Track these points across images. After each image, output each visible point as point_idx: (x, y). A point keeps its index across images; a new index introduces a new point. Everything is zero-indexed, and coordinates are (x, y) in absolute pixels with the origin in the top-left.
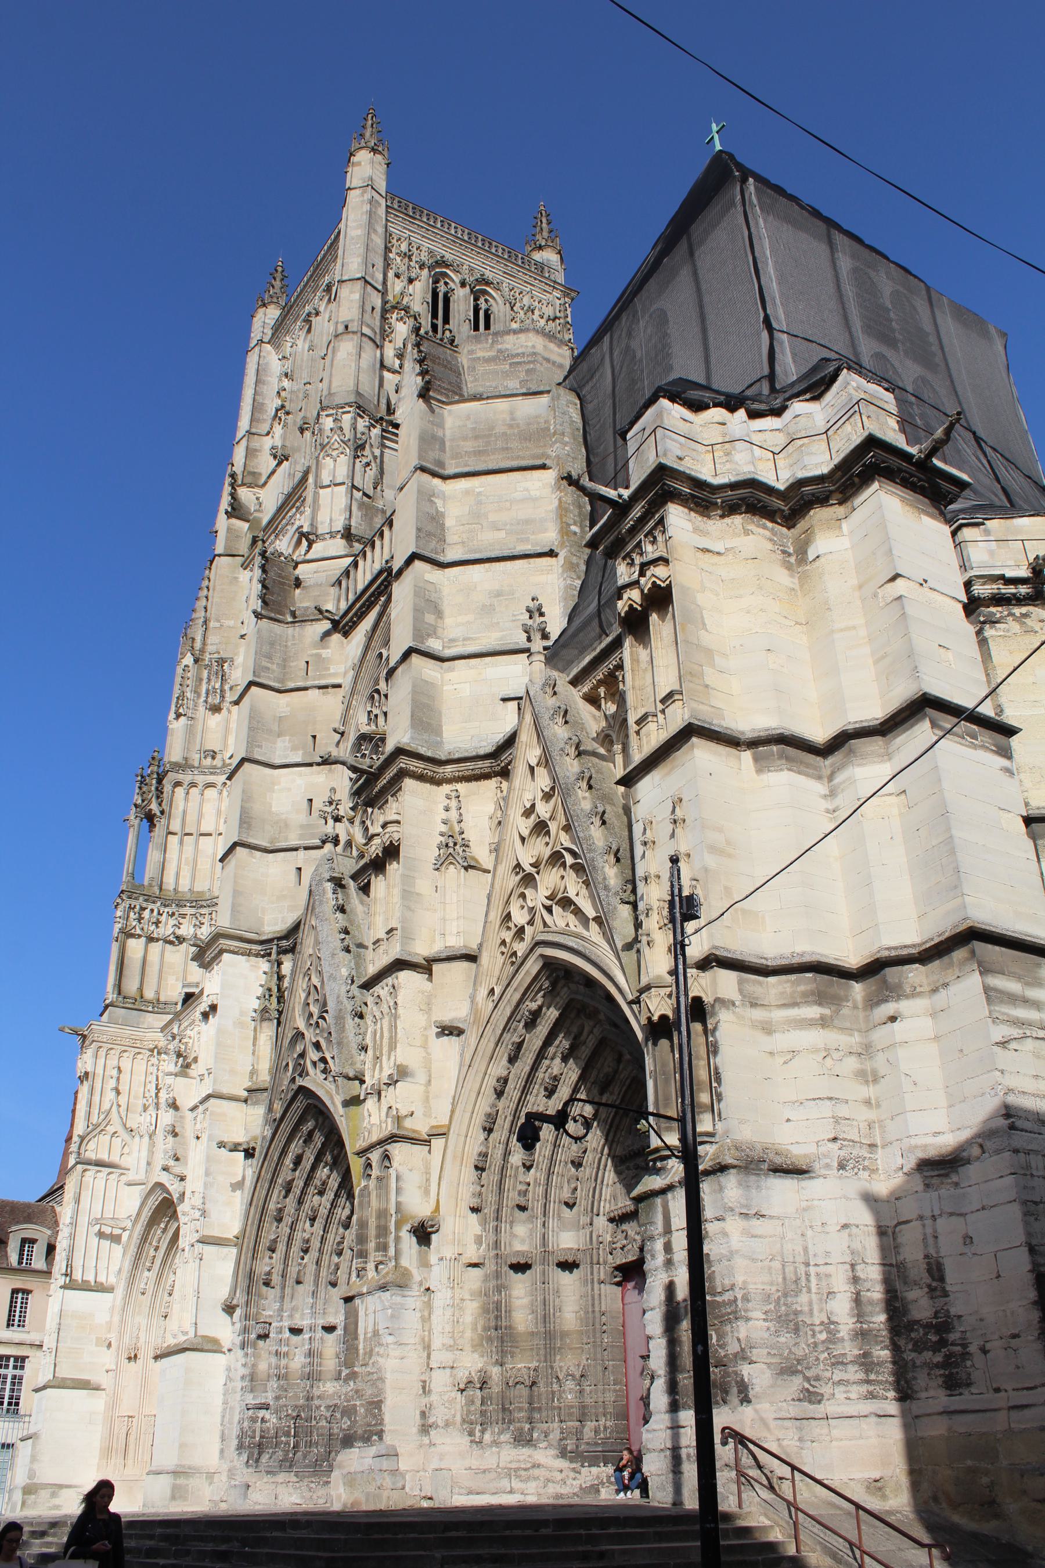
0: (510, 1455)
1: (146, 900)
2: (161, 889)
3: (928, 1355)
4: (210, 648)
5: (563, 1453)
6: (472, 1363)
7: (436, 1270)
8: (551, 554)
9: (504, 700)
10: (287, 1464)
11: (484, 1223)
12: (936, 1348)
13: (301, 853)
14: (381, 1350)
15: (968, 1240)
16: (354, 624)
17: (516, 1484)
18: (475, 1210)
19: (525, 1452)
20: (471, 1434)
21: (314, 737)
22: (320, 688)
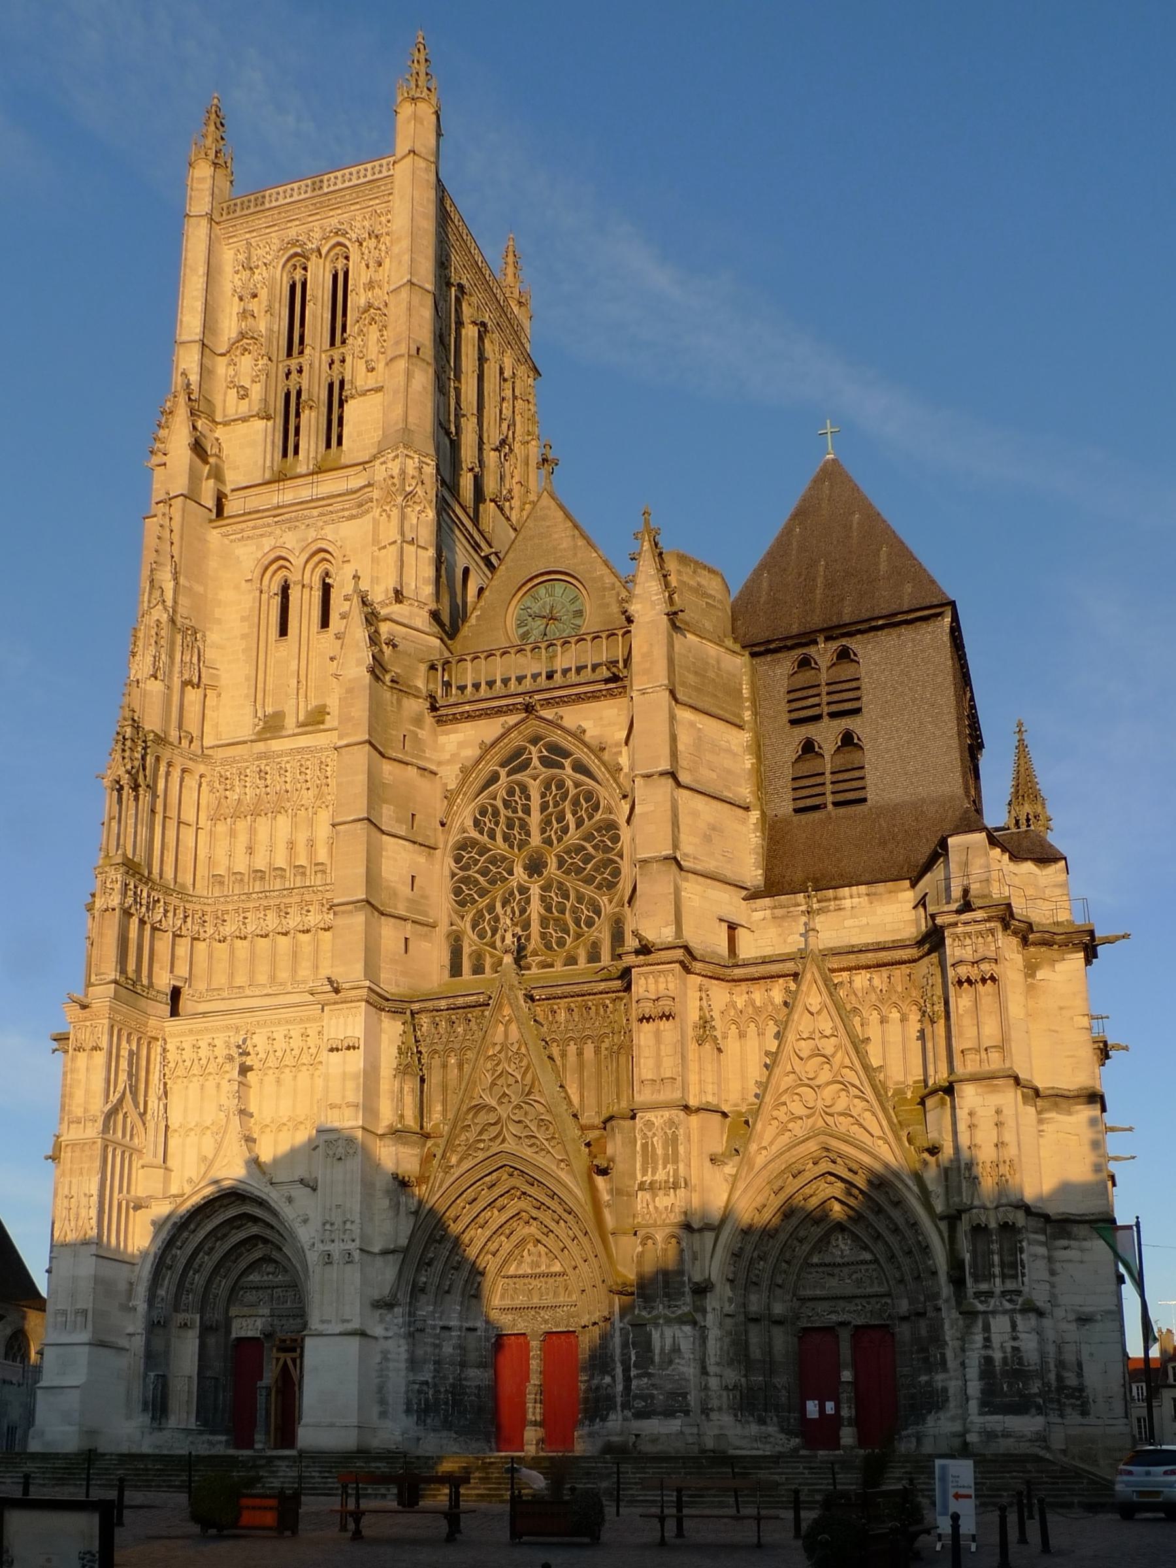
0: (754, 1429)
1: (140, 880)
2: (161, 878)
3: (1073, 1401)
4: (181, 610)
5: (782, 1430)
6: (732, 1376)
7: (710, 1317)
8: (747, 809)
9: (721, 920)
10: (447, 1425)
11: (733, 1289)
12: (1078, 1398)
13: (409, 925)
14: (683, 1362)
15: (1091, 1355)
16: (456, 719)
17: (760, 1445)
18: (731, 1281)
19: (763, 1428)
20: (736, 1415)
21: (413, 815)
22: (419, 768)
